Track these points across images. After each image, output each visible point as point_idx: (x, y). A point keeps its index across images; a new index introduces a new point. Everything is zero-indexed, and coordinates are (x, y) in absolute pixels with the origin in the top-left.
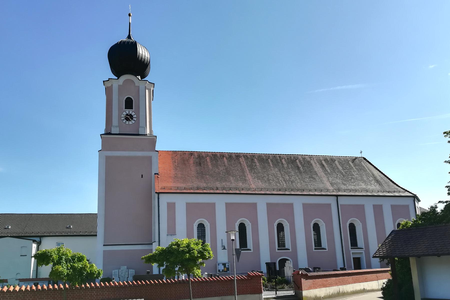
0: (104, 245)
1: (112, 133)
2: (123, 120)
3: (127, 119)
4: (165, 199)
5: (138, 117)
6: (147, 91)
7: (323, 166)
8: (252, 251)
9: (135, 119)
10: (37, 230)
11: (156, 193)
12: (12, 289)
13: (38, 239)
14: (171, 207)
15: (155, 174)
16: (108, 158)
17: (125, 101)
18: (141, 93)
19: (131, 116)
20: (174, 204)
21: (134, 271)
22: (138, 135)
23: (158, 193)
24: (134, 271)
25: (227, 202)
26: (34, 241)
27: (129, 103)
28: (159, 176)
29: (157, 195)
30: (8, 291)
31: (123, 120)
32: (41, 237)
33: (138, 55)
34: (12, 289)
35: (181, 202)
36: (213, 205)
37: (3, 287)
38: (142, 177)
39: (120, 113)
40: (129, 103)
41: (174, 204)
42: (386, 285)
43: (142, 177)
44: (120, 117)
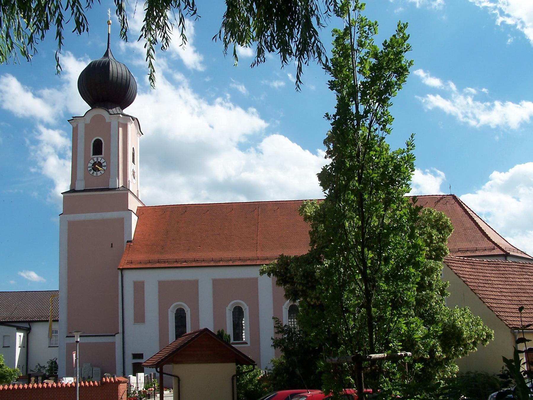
0: (67, 337)
1: (76, 189)
2: (90, 170)
3: (95, 170)
4: (130, 277)
5: (108, 166)
6: (121, 129)
7: (165, 262)
8: (249, 345)
9: (91, 173)
10: (29, 313)
11: (119, 269)
12: (16, 387)
13: (27, 325)
14: (139, 287)
15: (128, 242)
16: (71, 225)
17: (94, 142)
18: (113, 132)
19: (100, 164)
20: (143, 283)
21: (99, 369)
22: (109, 189)
23: (122, 270)
24: (99, 369)
25: (199, 281)
26: (19, 329)
27: (98, 148)
28: (132, 244)
29: (120, 272)
30: (9, 389)
31: (90, 170)
32: (29, 322)
33: (110, 78)
34: (11, 387)
35: (152, 279)
36: (196, 283)
37: (4, 386)
38: (112, 247)
39: (87, 161)
40: (98, 148)
41: (143, 283)
42: (403, 394)
43: (112, 247)
44: (86, 167)
